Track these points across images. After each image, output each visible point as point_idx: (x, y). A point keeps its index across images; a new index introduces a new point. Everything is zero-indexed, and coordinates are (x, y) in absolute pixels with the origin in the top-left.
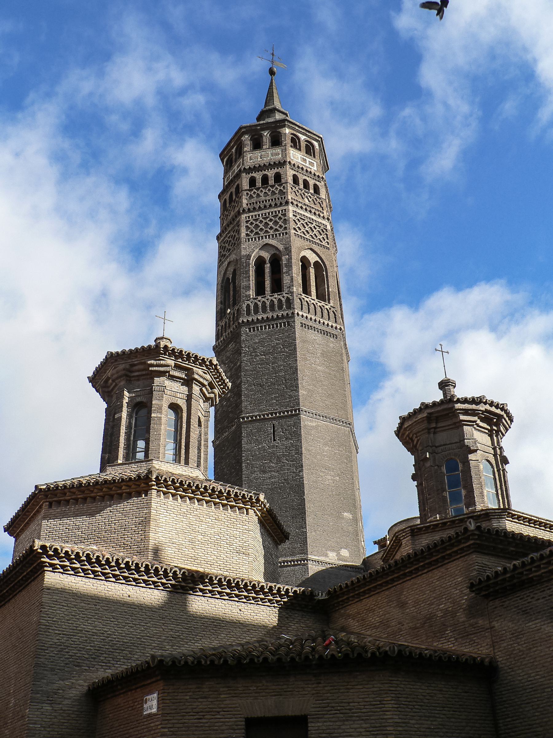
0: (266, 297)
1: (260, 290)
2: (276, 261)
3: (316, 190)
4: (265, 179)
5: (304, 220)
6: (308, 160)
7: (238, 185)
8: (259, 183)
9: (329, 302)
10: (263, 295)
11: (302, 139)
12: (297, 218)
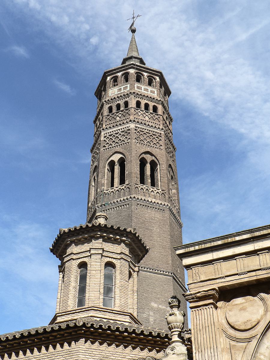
0: (113, 188)
2: (122, 162)
4: (118, 106)
7: (102, 113)
11: (146, 75)
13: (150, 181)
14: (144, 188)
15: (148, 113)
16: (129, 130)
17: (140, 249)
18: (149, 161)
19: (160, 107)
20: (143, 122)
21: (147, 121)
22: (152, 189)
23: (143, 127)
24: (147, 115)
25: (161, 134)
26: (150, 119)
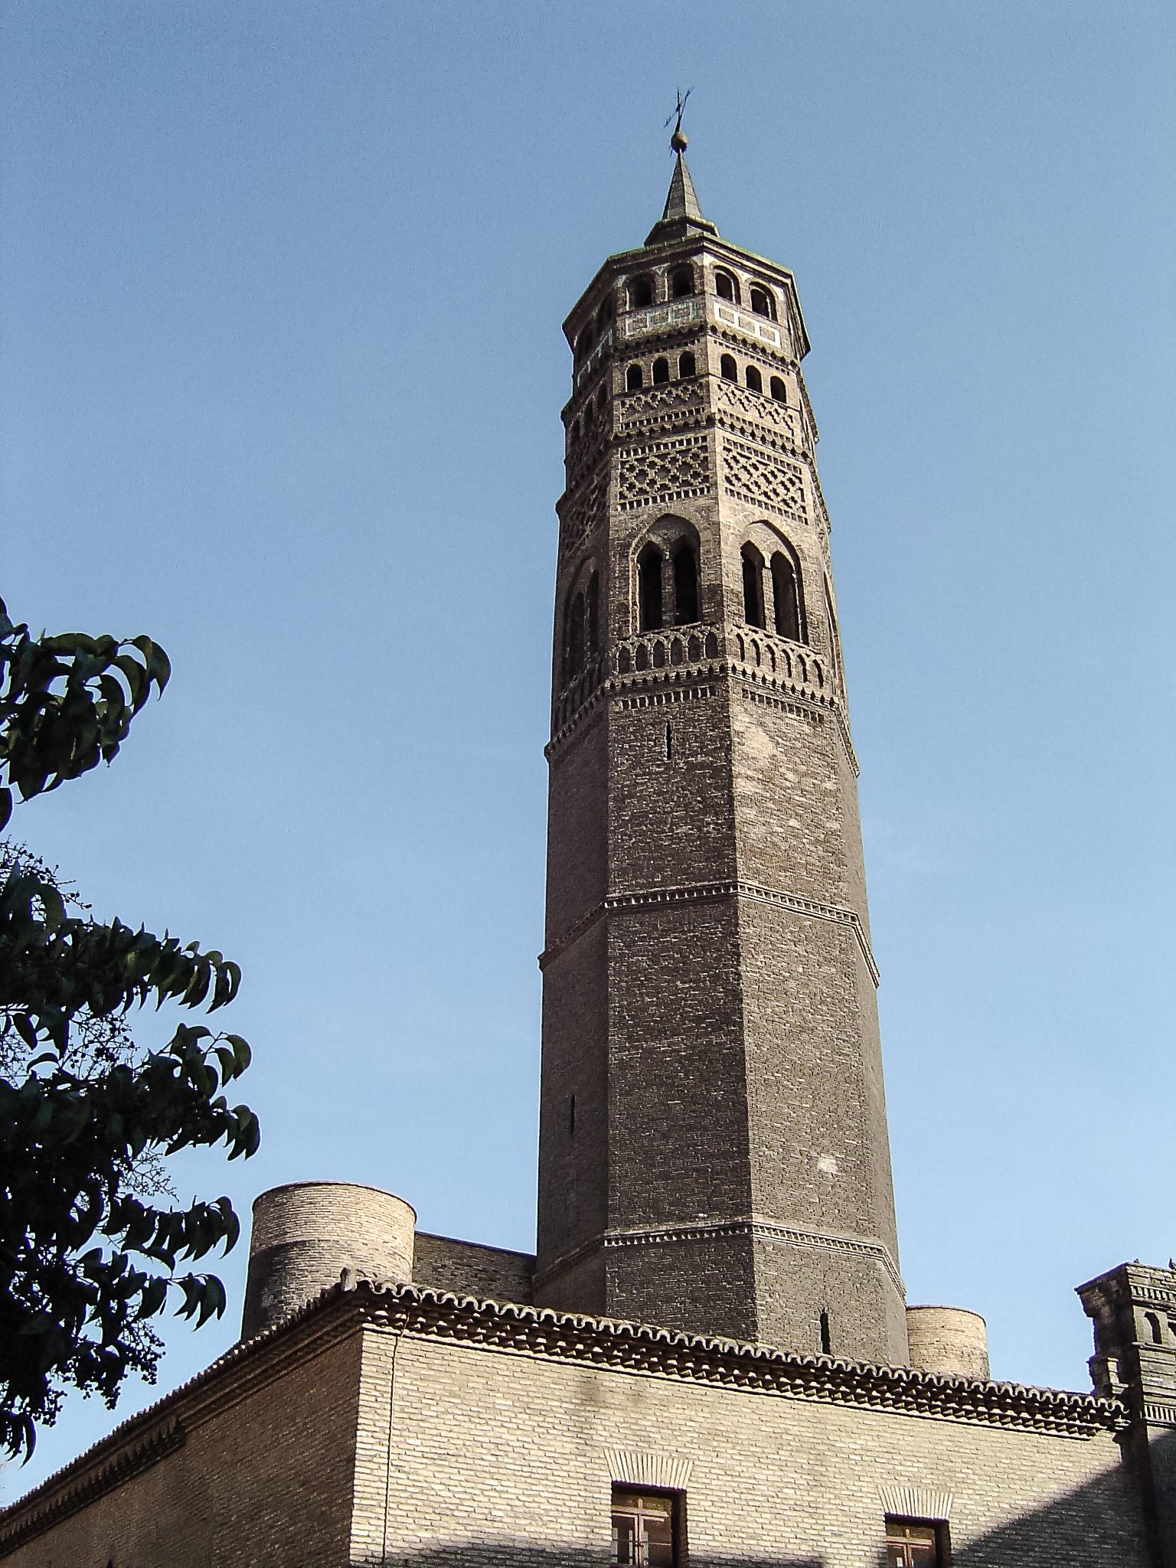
1: (652, 621)
3: (778, 390)
4: (661, 367)
5: (749, 458)
6: (757, 325)
8: (648, 379)
10: (657, 629)
11: (743, 280)
12: (731, 454)
19: (790, 381)
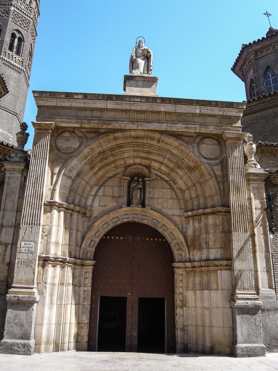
9: (21, 57)
13: (15, 50)
14: (10, 54)
15: (25, 3)
16: (9, 10)
17: (3, 89)
18: (17, 37)
20: (20, 9)
21: (23, 9)
22: (15, 56)
23: (19, 12)
24: (24, 5)
25: (30, 21)
26: (25, 8)
